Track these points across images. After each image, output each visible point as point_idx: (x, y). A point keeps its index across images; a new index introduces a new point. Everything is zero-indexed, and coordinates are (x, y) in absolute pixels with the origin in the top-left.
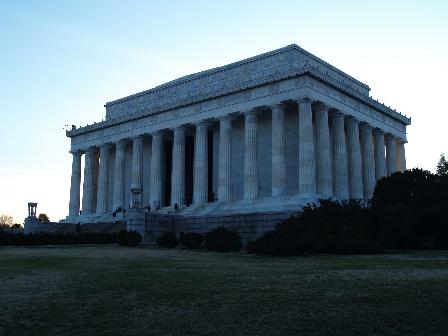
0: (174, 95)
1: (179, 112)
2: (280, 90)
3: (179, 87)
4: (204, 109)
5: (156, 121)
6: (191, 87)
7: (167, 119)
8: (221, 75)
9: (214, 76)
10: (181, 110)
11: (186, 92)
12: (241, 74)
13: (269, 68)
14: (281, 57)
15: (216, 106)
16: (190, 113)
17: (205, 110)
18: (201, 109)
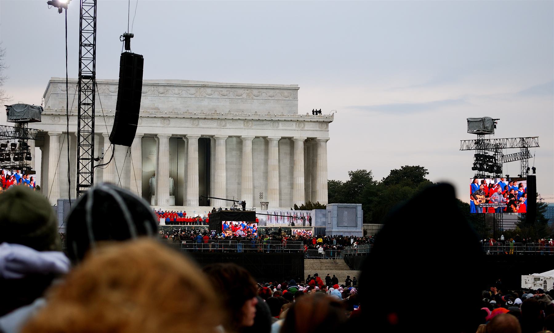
0: (162, 95)
1: (198, 122)
2: (306, 128)
3: (167, 88)
4: (228, 126)
5: (169, 124)
6: (184, 92)
7: (183, 126)
8: (222, 91)
9: (214, 89)
10: (201, 121)
11: (177, 96)
12: (244, 96)
13: (273, 98)
14: (286, 93)
15: (242, 126)
16: (211, 126)
17: (230, 127)
18: (225, 125)
